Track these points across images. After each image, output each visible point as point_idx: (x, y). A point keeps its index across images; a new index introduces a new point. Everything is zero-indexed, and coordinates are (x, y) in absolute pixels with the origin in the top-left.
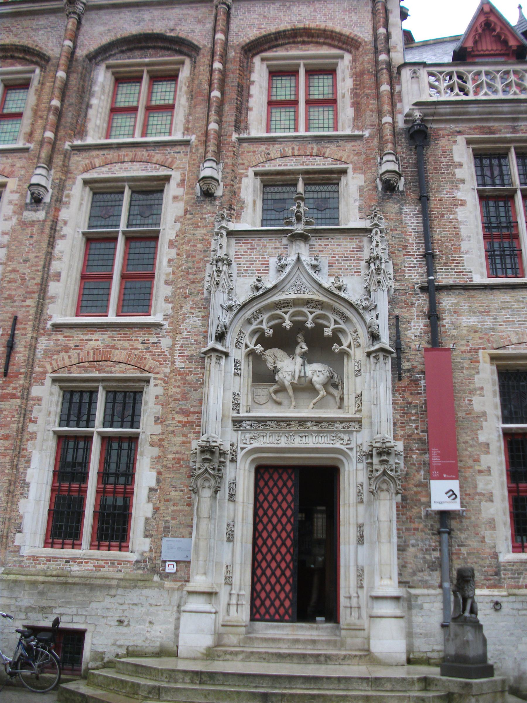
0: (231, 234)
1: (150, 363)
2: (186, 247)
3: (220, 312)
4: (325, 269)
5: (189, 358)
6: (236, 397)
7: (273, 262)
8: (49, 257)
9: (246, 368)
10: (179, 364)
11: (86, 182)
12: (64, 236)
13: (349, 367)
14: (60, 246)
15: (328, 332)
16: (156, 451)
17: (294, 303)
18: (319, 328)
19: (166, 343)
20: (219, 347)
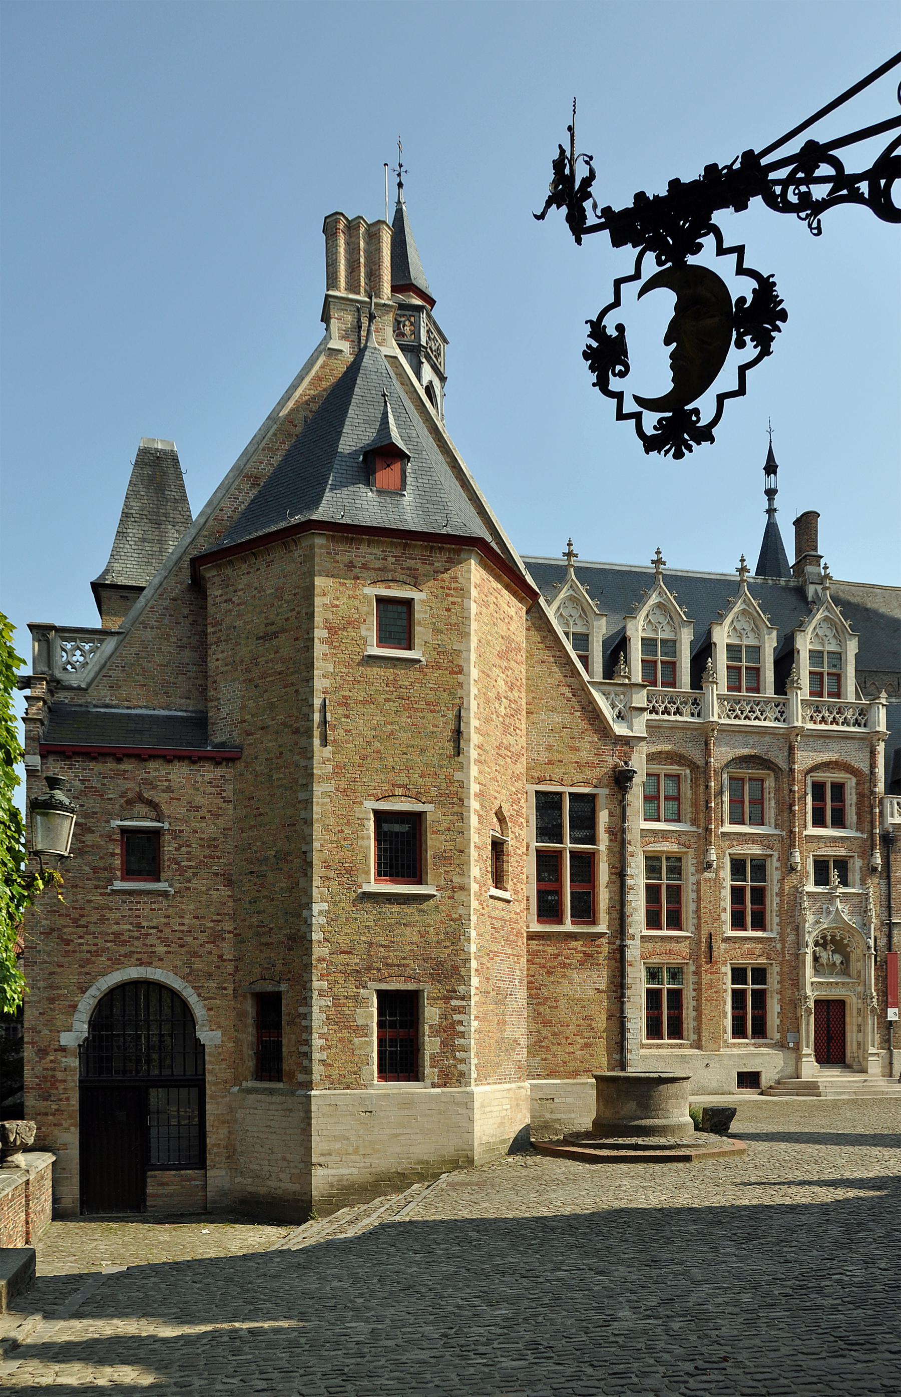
18: (842, 939)
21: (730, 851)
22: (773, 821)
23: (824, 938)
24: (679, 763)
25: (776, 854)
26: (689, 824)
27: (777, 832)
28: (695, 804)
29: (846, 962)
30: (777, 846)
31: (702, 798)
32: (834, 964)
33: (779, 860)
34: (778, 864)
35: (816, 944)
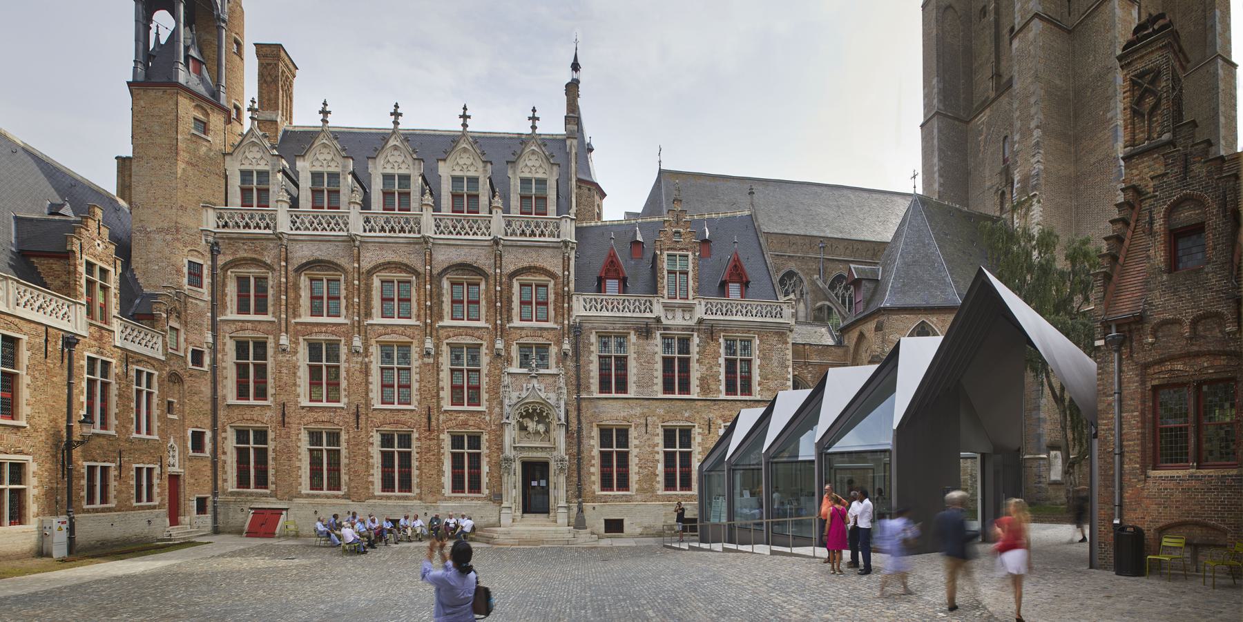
0: (508, 374)
1: (483, 426)
2: (492, 378)
3: (507, 407)
4: (543, 390)
5: (497, 425)
6: (514, 438)
7: (525, 385)
8: (438, 380)
9: (517, 427)
10: (493, 428)
11: (447, 344)
12: (442, 370)
13: (552, 427)
14: (442, 375)
15: (544, 414)
16: (488, 459)
17: (533, 402)
18: (542, 412)
19: (488, 418)
20: (507, 421)
21: (447, 341)
22: (484, 317)
23: (527, 411)
24: (406, 271)
25: (485, 343)
26: (415, 319)
27: (487, 325)
28: (419, 304)
29: (547, 431)
30: (486, 336)
31: (422, 298)
32: (537, 433)
33: (487, 348)
34: (487, 351)
35: (522, 416)
